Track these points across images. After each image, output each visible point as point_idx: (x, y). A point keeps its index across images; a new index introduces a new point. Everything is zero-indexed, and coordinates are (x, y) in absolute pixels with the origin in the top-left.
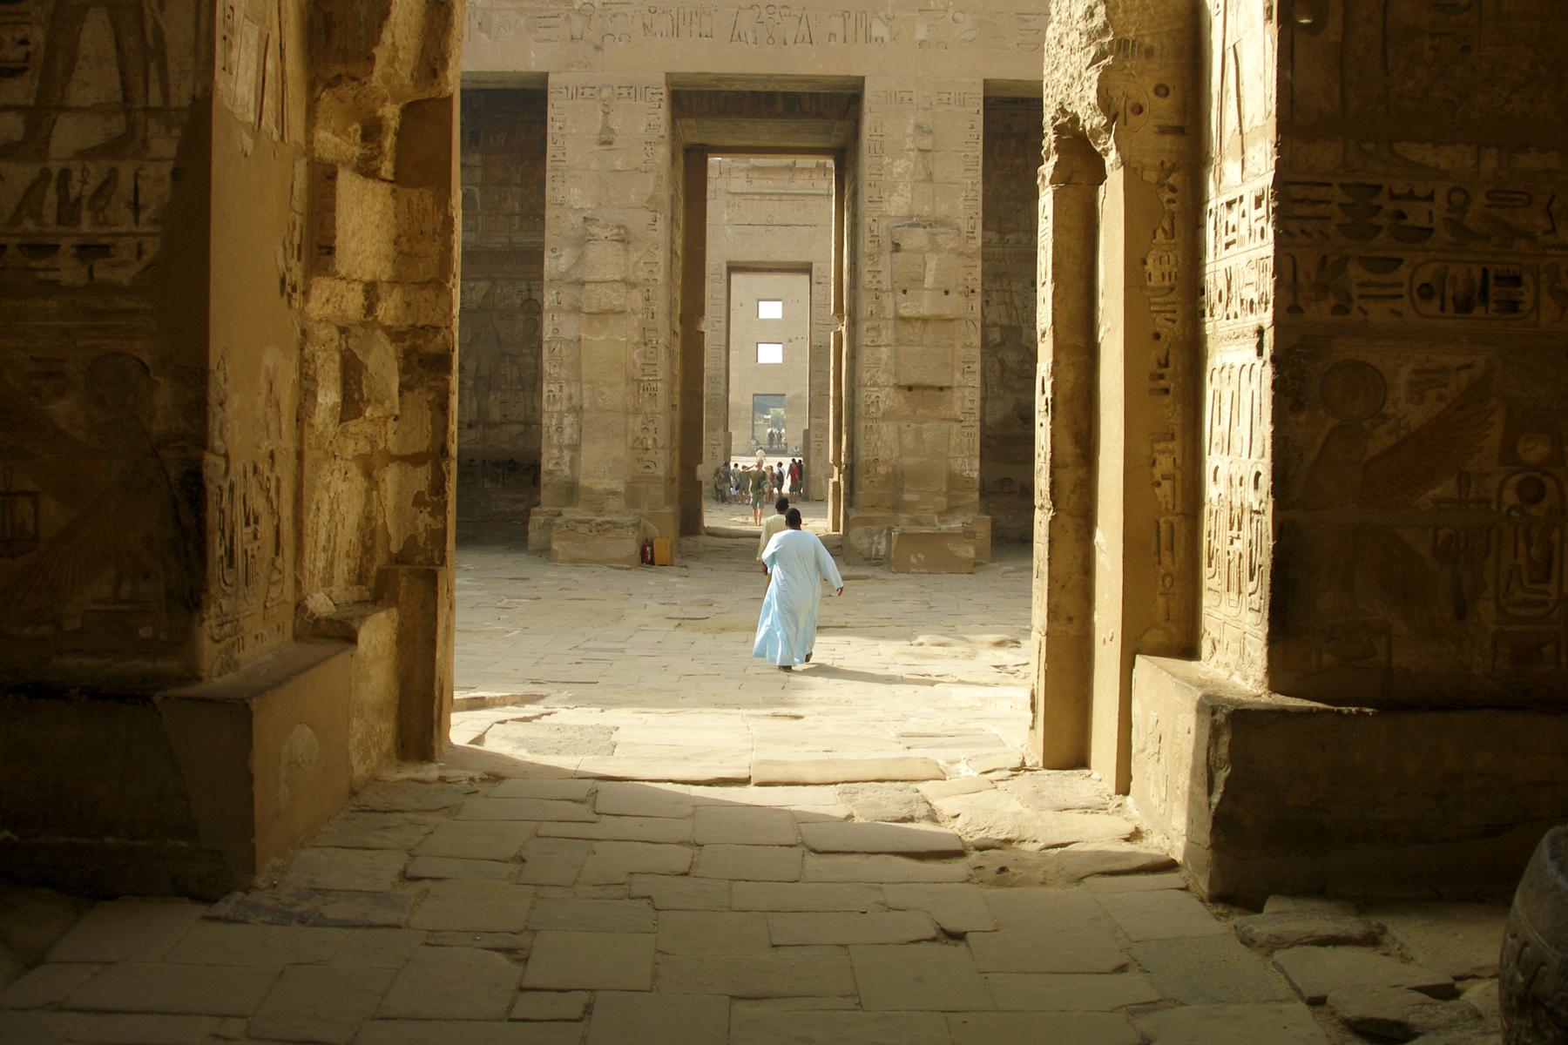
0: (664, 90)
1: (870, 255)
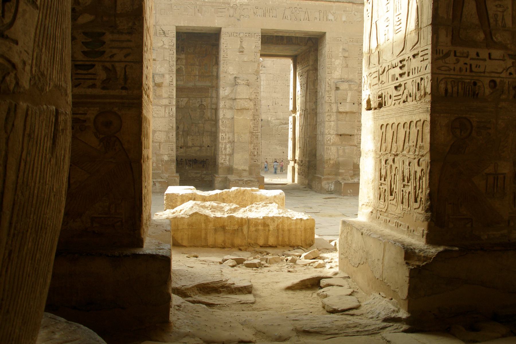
1: (328, 91)
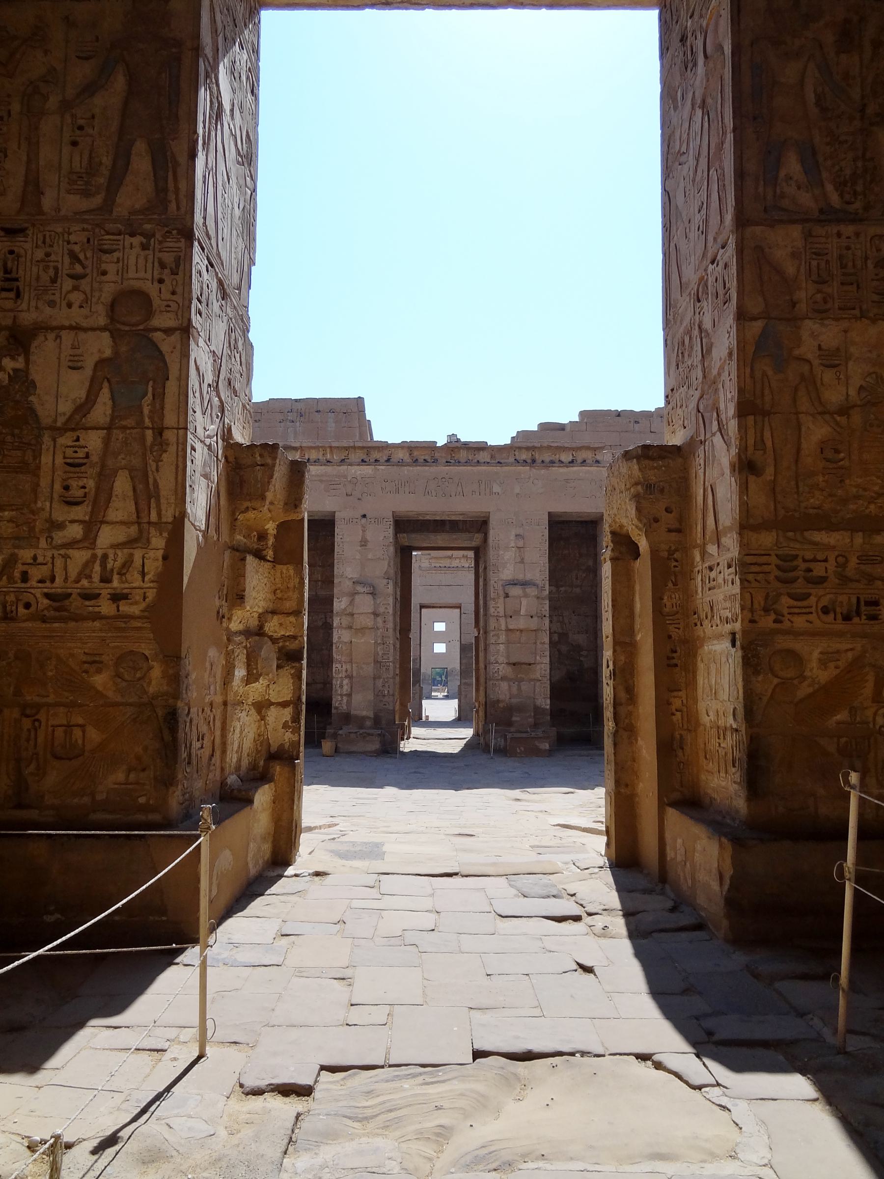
0: (392, 520)
